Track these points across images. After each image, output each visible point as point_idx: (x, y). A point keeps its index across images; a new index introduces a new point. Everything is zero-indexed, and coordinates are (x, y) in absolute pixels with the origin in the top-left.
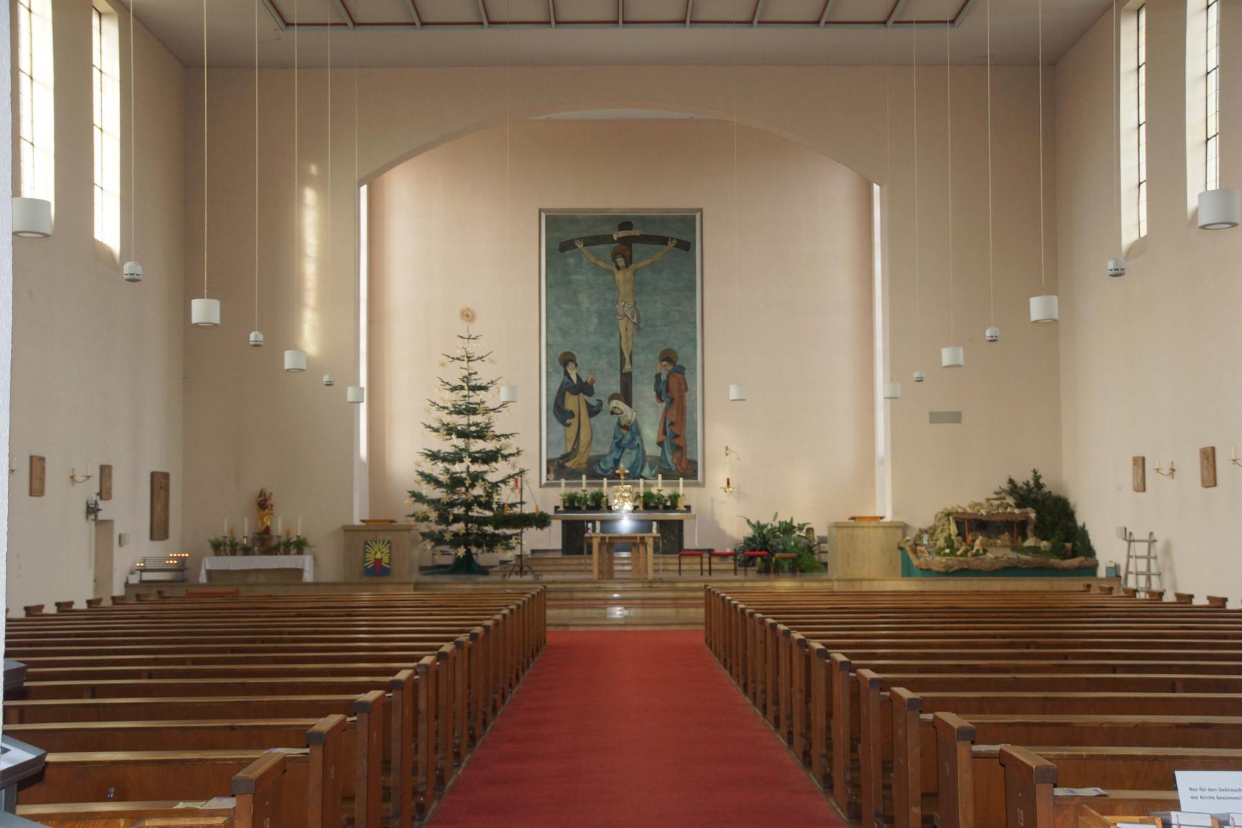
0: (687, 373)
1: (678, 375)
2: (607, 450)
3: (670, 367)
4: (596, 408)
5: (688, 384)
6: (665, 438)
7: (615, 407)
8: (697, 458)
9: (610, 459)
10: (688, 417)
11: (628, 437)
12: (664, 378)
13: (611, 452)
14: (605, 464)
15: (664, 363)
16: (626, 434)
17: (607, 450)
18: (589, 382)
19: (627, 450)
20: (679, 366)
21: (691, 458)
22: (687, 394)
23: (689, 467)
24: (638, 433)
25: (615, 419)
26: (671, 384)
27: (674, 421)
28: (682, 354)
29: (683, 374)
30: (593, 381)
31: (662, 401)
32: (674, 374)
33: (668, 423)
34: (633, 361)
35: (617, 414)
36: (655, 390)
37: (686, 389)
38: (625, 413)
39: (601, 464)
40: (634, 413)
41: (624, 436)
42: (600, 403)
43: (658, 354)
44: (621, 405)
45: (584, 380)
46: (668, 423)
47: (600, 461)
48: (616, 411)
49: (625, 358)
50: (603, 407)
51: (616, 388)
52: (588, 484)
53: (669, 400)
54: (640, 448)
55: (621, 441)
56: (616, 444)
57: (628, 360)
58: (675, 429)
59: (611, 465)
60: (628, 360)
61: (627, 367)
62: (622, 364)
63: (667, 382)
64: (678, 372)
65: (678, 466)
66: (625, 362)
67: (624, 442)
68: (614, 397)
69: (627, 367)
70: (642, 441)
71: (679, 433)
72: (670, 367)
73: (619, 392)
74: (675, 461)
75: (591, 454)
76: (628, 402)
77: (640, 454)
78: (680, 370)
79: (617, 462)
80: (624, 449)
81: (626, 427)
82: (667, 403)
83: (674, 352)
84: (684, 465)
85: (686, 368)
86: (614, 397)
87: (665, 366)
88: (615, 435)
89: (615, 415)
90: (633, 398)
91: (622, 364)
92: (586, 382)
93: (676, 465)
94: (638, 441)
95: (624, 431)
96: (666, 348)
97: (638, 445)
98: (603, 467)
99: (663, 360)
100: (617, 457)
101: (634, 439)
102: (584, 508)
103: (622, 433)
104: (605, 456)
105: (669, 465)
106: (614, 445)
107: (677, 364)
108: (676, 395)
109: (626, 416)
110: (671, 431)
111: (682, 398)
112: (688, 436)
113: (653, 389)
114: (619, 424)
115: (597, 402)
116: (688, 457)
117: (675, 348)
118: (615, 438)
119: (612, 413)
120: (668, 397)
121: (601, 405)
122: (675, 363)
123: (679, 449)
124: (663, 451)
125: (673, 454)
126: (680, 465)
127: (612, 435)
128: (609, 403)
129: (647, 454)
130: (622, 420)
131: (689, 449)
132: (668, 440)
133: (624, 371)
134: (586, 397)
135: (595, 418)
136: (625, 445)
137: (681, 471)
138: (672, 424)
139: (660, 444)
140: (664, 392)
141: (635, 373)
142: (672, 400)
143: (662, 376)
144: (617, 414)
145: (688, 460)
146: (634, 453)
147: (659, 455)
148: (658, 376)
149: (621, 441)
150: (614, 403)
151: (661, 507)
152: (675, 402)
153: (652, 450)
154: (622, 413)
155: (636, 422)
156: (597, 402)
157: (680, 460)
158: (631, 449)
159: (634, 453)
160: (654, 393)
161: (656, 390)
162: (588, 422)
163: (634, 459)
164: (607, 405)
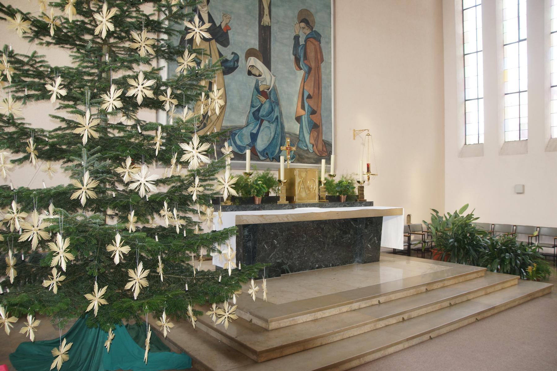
0: (323, 40)
1: (316, 43)
2: (242, 121)
3: (308, 31)
4: (232, 64)
5: (324, 54)
6: (302, 112)
7: (253, 66)
8: (332, 139)
9: (246, 132)
10: (323, 92)
11: (267, 106)
12: (302, 41)
13: (248, 125)
14: (241, 140)
15: (303, 25)
16: (265, 103)
17: (242, 121)
18: (223, 27)
19: (265, 123)
20: (315, 31)
21: (326, 139)
22: (323, 65)
23: (325, 149)
24: (276, 103)
25: (252, 81)
26: (308, 51)
27: (311, 94)
28: (318, 18)
29: (320, 42)
30: (228, 28)
31: (301, 69)
32: (312, 40)
33: (305, 97)
34: (272, 14)
35: (255, 75)
36: (293, 54)
37: (322, 60)
38: (263, 76)
39: (236, 137)
40: (273, 78)
41: (262, 105)
42: (236, 59)
43: (297, 12)
44: (260, 65)
45: (218, 25)
46: (305, 97)
47: (236, 134)
48: (254, 71)
49: (264, 8)
50: (240, 64)
51: (254, 43)
52: (252, 167)
53: (306, 69)
54: (278, 121)
55: (259, 110)
56: (254, 114)
57: (266, 11)
58: (312, 102)
59: (247, 140)
60: (266, 11)
61: (266, 20)
62: (261, 16)
63: (305, 46)
64: (314, 38)
65: (315, 147)
66: (264, 12)
67: (263, 112)
68: (250, 53)
69: (266, 20)
70: (281, 113)
71: (316, 109)
72: (308, 31)
73: (257, 47)
74: (313, 142)
75: (226, 124)
76: (267, 63)
77: (279, 130)
78: (315, 37)
79: (254, 137)
80: (262, 121)
81: (264, 94)
82: (306, 73)
83: (311, 15)
84: (320, 147)
85: (322, 36)
86: (250, 53)
87: (304, 28)
88: (252, 102)
89: (252, 76)
90: (272, 59)
91: (261, 16)
92: (220, 25)
93: (313, 146)
94: (276, 114)
95: (263, 99)
96: (305, 8)
97: (277, 118)
98: (239, 143)
99: (301, 22)
100: (255, 131)
101: (273, 110)
102: (258, 200)
103: (260, 101)
104: (241, 128)
105: (307, 146)
106: (251, 114)
107: (314, 30)
108: (313, 65)
109: (265, 79)
110: (309, 105)
111: (318, 68)
112: (324, 114)
113: (292, 52)
114: (257, 88)
115: (233, 55)
116: (323, 138)
117: (312, 11)
118: (252, 106)
119: (250, 73)
120: (306, 65)
121: (237, 61)
122: (312, 28)
123: (315, 127)
124: (301, 128)
125: (310, 132)
126: (317, 147)
127: (249, 103)
128: (247, 58)
129: (286, 130)
130: (260, 84)
131: (324, 128)
132: (306, 116)
133: (262, 24)
134: (219, 46)
135: (230, 76)
136: (263, 116)
137: (318, 154)
138: (309, 97)
139: (299, 119)
140: (302, 59)
141: (274, 29)
142: (310, 69)
143: (300, 39)
144: (255, 75)
145: (323, 140)
146: (273, 126)
147: (298, 133)
148: (297, 38)
149: (259, 110)
150: (253, 61)
151: (343, 198)
152: (313, 71)
153: (292, 127)
154: (260, 76)
155: (275, 89)
156: (233, 55)
157: (317, 139)
158: (269, 122)
159: (273, 126)
160: (293, 57)
161: (296, 54)
162: (221, 80)
163: (272, 135)
164: (244, 61)
